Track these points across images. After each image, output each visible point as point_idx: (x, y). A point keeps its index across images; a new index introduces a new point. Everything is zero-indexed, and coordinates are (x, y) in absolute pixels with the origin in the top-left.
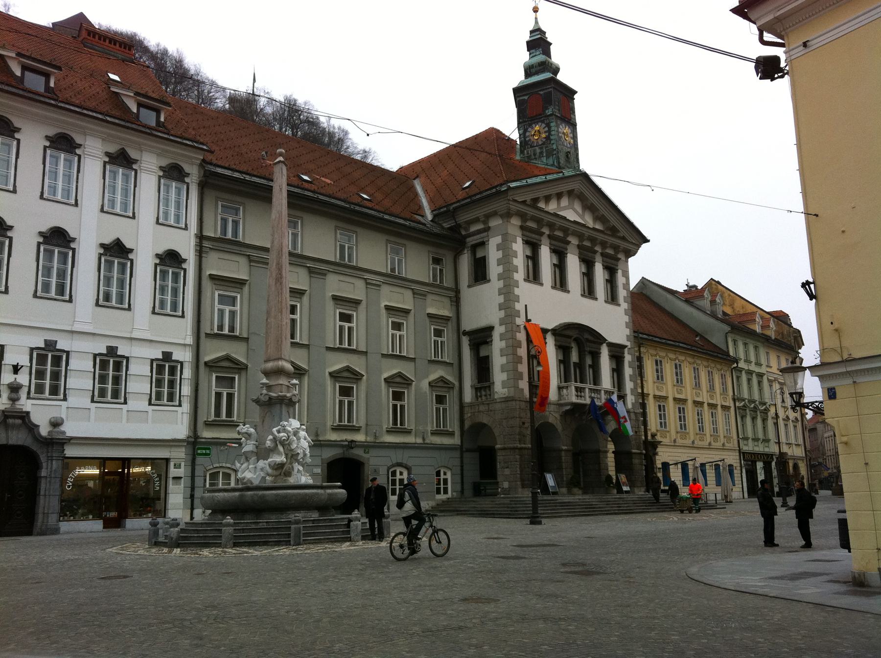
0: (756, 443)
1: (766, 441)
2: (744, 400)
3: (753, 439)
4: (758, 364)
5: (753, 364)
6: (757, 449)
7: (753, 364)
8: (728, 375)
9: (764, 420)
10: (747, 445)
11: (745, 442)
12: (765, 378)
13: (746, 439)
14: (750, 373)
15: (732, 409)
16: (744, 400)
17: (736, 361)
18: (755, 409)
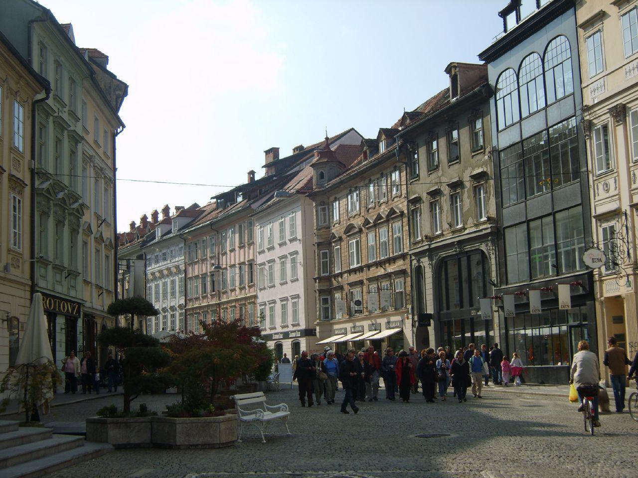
0: (58, 277)
1: (72, 274)
2: (48, 179)
3: (55, 267)
4: (72, 114)
5: (66, 110)
6: (59, 289)
7: (66, 110)
8: (28, 107)
9: (74, 232)
10: (44, 277)
11: (43, 271)
12: (80, 146)
13: (44, 262)
14: (61, 125)
15: (27, 191)
16: (45, 176)
17: (44, 85)
18: (62, 205)
